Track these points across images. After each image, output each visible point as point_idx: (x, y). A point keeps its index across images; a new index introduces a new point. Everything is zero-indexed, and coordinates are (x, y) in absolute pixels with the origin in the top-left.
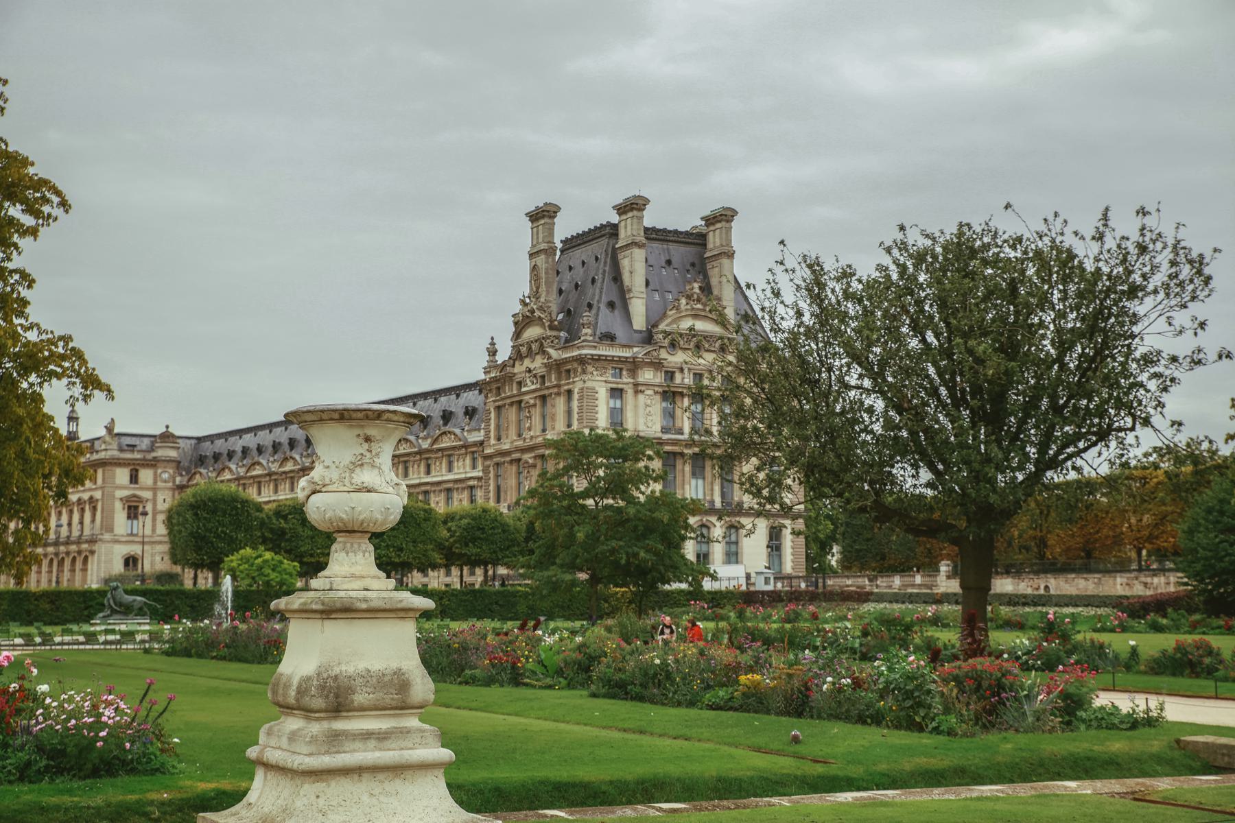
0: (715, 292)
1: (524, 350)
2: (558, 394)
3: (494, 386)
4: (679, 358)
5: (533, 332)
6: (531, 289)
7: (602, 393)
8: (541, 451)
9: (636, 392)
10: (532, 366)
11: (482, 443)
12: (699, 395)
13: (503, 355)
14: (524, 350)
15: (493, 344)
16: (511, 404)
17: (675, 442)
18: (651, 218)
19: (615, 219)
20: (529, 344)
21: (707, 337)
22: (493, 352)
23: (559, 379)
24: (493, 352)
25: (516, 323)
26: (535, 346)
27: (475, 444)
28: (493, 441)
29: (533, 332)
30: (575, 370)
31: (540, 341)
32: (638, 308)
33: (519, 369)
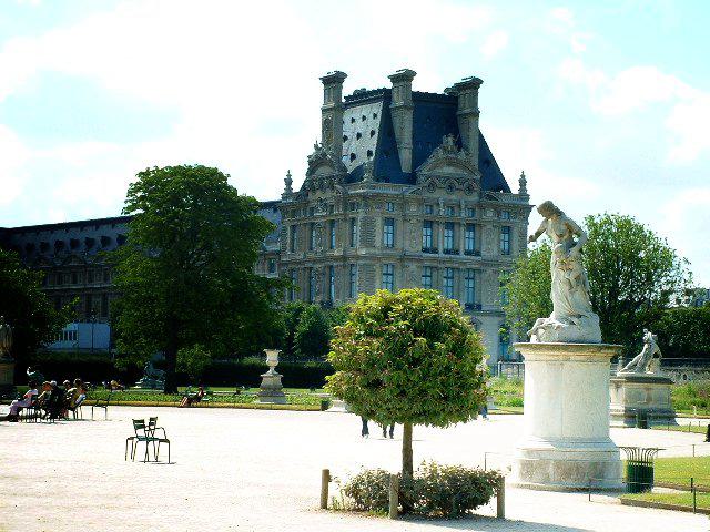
1: (316, 184)
5: (324, 171)
6: (323, 137)
7: (379, 222)
9: (404, 220)
11: (278, 253)
12: (450, 225)
13: (297, 187)
14: (316, 184)
17: (435, 260)
18: (418, 85)
19: (389, 85)
21: (460, 180)
22: (289, 182)
23: (346, 210)
24: (289, 182)
25: (310, 163)
29: (324, 171)
30: (358, 204)
31: (330, 178)
32: (406, 155)
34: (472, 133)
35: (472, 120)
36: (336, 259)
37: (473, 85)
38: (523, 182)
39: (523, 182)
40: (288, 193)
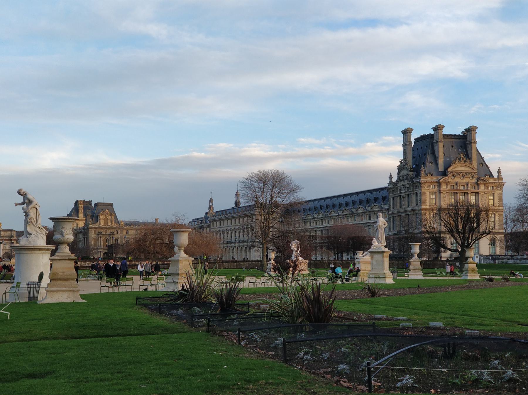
0: (470, 156)
2: (413, 194)
3: (392, 190)
4: (457, 180)
8: (408, 213)
10: (404, 184)
11: (388, 209)
14: (401, 178)
15: (391, 175)
16: (398, 196)
19: (432, 132)
20: (403, 176)
22: (391, 178)
23: (413, 189)
24: (391, 178)
26: (405, 177)
27: (385, 209)
28: (391, 209)
29: (404, 172)
33: (400, 184)
34: (474, 151)
35: (473, 145)
36: (410, 211)
37: (471, 131)
38: (499, 172)
39: (499, 172)
40: (391, 182)
